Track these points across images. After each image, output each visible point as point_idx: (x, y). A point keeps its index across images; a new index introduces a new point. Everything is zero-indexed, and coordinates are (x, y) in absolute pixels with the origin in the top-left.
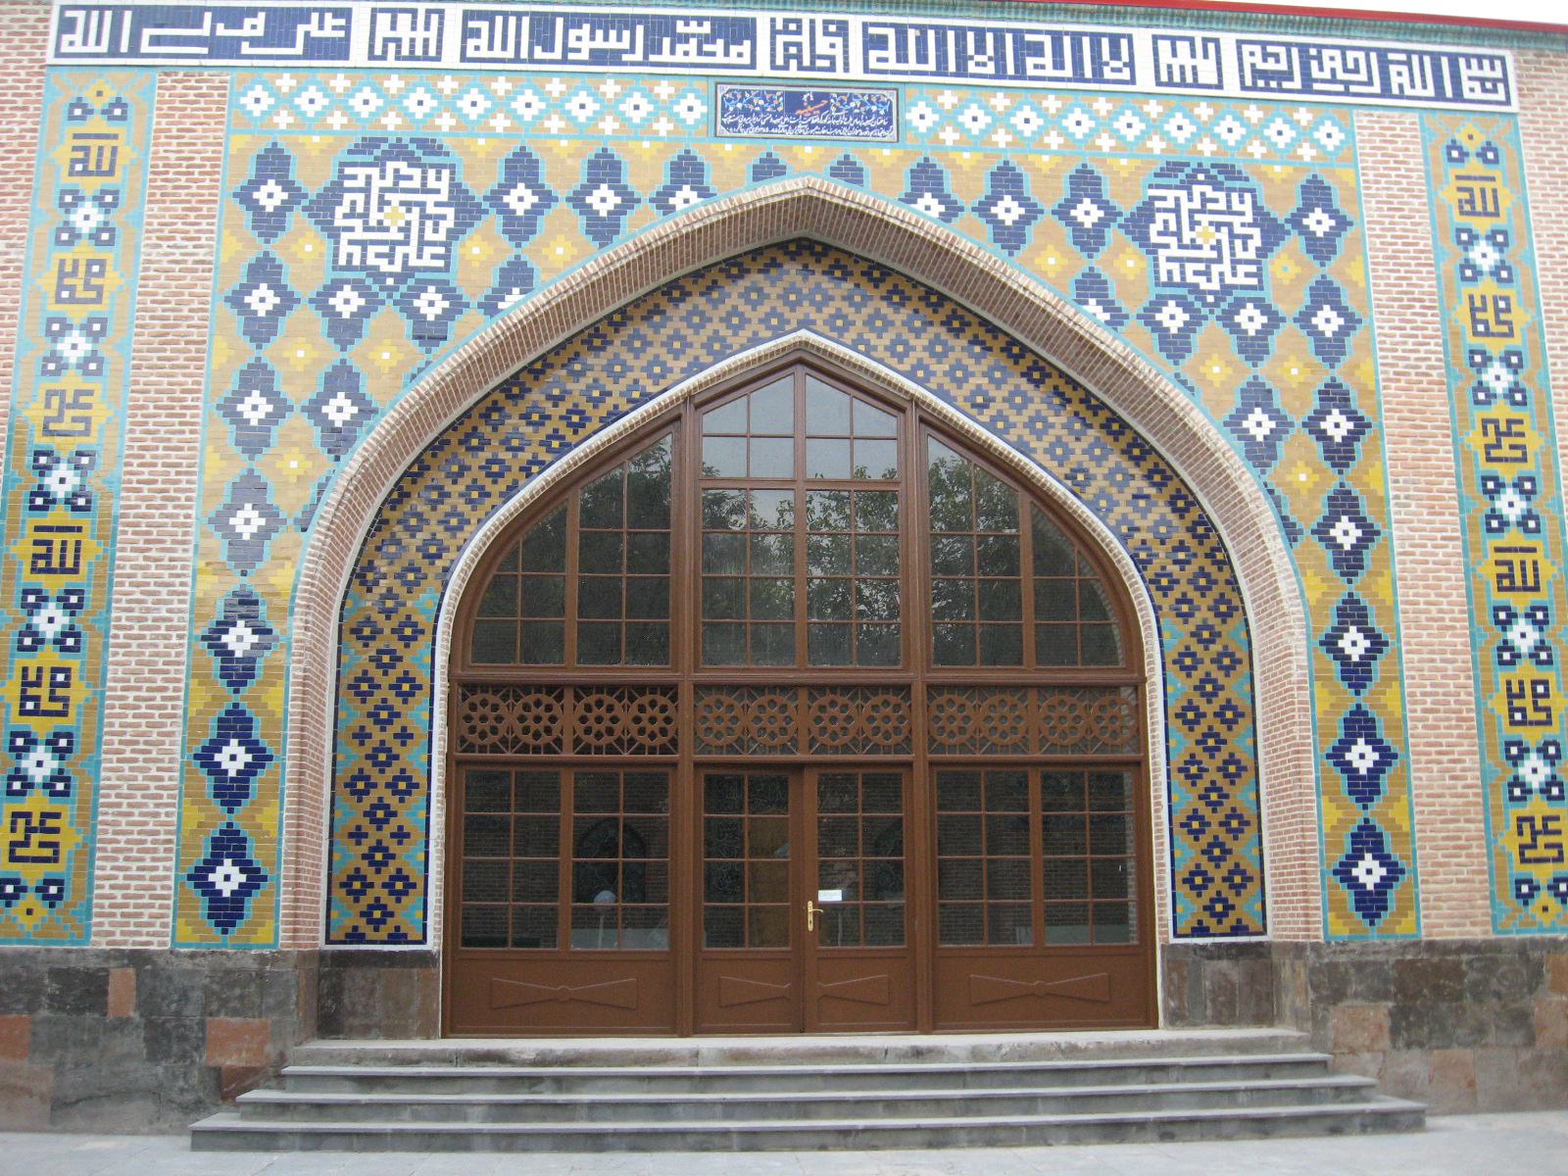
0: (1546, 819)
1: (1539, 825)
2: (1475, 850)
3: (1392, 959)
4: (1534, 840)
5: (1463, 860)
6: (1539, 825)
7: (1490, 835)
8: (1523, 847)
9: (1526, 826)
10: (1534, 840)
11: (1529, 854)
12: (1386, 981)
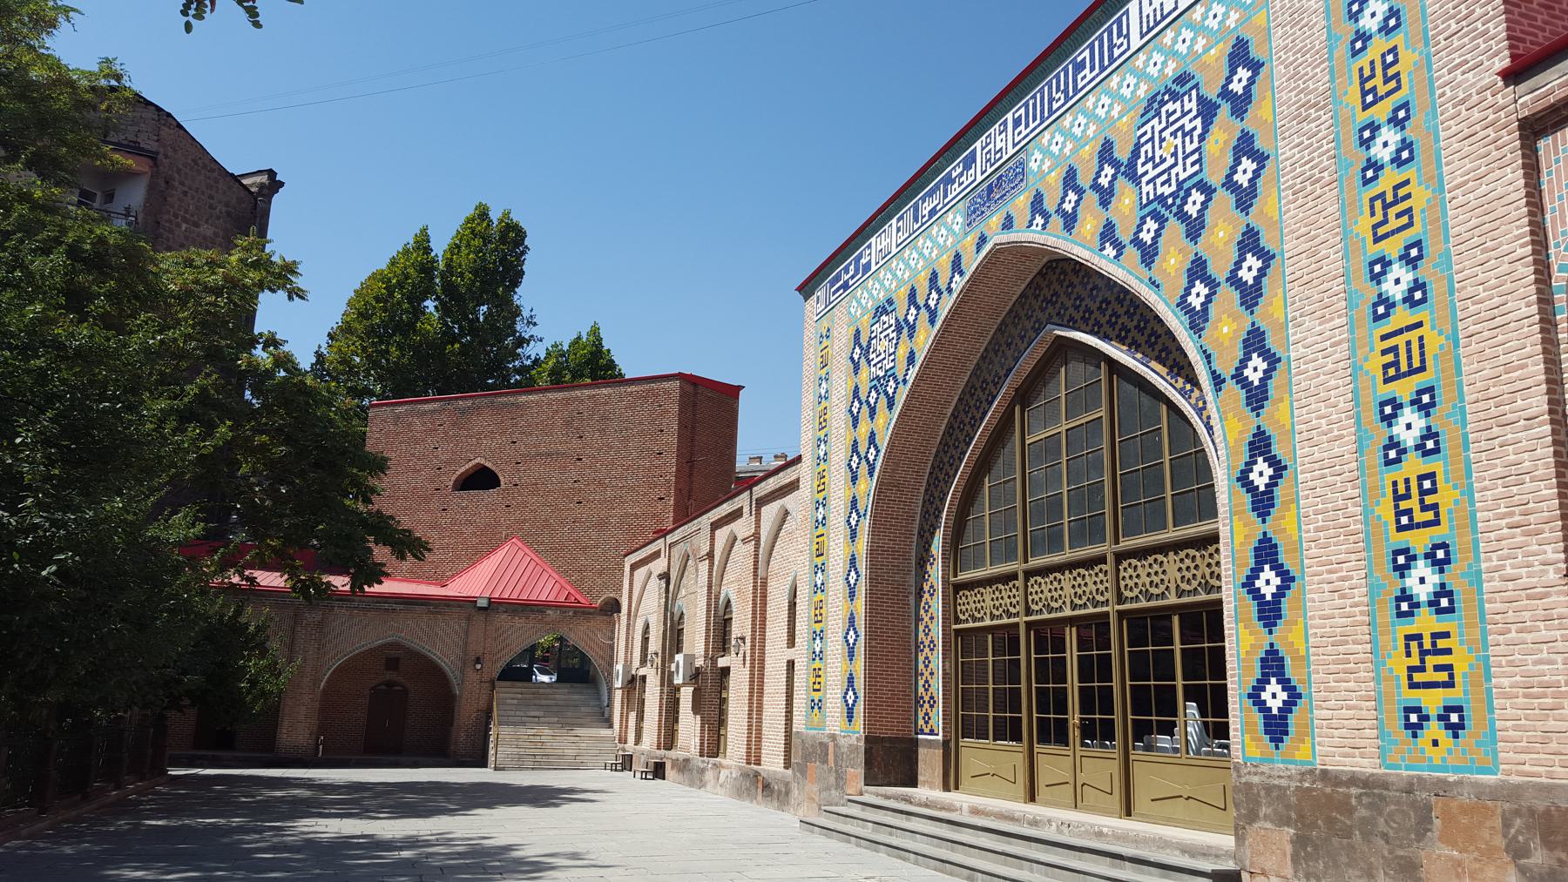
0: (1435, 636)
1: (1427, 645)
2: (1362, 674)
3: (1294, 784)
4: (1422, 661)
5: (1352, 685)
6: (1427, 645)
7: (1377, 653)
8: (1411, 669)
9: (1414, 645)
10: (1422, 661)
11: (1418, 677)
12: (1288, 807)
